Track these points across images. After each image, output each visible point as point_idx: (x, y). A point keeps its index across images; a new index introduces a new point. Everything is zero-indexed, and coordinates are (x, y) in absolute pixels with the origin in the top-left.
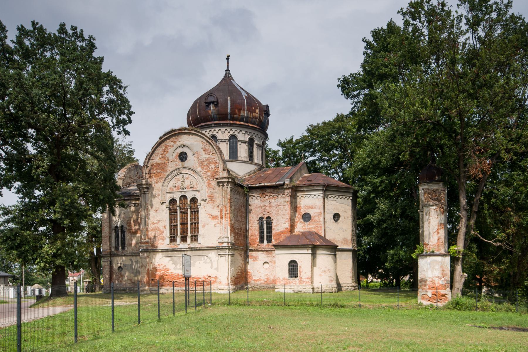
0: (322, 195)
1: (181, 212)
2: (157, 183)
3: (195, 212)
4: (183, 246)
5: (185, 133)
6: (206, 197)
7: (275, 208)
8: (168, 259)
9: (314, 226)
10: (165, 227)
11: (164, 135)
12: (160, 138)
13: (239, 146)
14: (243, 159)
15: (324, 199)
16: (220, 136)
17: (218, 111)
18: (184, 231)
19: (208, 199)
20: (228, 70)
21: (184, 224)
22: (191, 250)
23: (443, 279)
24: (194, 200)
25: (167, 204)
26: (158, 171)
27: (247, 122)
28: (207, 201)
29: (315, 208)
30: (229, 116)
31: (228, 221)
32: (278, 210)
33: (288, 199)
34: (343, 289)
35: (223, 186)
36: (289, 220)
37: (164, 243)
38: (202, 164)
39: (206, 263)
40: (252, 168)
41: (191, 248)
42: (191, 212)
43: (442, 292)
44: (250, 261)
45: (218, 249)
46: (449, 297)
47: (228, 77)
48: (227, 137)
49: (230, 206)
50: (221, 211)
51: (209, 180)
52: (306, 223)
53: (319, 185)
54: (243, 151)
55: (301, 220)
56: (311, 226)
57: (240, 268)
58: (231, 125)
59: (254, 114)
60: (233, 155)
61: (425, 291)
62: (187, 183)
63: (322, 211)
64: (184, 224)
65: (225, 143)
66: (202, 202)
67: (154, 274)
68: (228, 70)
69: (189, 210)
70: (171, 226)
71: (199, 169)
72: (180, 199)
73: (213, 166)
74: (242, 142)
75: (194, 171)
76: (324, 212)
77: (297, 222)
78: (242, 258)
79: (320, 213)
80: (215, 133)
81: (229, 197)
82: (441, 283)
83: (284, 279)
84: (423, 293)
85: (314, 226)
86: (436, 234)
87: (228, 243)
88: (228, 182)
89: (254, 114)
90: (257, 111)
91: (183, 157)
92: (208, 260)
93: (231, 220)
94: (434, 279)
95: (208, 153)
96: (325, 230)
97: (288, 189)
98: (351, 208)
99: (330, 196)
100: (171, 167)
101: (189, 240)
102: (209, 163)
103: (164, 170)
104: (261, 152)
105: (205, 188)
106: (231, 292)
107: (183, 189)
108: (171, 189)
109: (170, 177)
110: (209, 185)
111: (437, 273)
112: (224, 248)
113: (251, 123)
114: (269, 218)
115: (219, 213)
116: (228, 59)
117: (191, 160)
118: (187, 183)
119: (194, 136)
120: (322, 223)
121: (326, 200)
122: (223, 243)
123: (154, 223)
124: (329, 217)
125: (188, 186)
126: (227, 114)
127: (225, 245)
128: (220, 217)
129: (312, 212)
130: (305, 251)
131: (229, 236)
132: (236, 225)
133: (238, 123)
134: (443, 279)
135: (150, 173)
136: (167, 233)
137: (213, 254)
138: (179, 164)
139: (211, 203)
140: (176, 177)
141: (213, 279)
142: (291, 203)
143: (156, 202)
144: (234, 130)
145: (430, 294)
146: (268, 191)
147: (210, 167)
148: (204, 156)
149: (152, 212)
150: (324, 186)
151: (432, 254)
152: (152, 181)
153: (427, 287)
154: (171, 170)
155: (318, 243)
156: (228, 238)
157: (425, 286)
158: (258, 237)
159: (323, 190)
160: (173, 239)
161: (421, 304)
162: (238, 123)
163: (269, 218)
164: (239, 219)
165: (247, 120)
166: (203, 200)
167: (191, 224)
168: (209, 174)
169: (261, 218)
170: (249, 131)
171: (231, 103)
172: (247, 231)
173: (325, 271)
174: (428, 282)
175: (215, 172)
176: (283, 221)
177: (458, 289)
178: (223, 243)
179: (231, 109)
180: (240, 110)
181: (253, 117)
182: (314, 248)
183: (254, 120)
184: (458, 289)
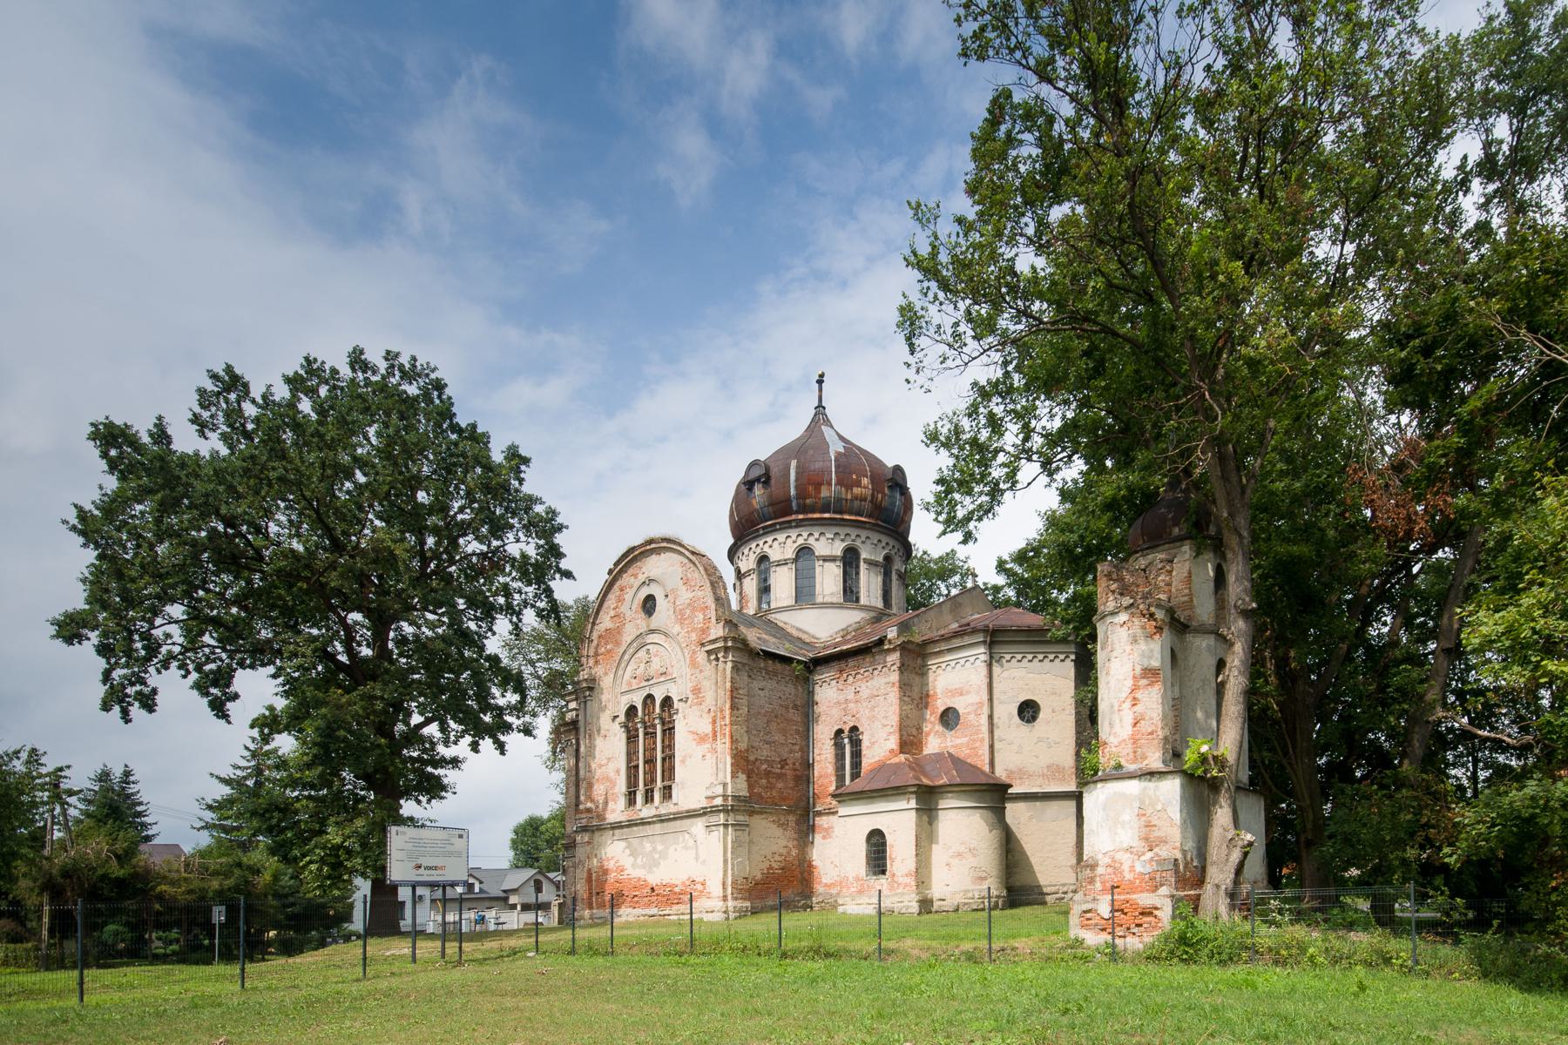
0: (983, 657)
1: (646, 734)
3: (669, 731)
4: (647, 812)
5: (653, 551)
7: (864, 705)
8: (623, 844)
9: (965, 740)
10: (618, 771)
11: (616, 565)
12: (610, 572)
13: (818, 569)
14: (835, 600)
15: (990, 666)
16: (775, 554)
17: (770, 496)
20: (820, 406)
21: (650, 761)
22: (662, 819)
23: (1149, 855)
24: (667, 702)
25: (622, 718)
27: (841, 512)
29: (968, 692)
30: (794, 504)
31: (728, 745)
32: (873, 708)
33: (895, 677)
34: (1048, 898)
35: (717, 659)
36: (896, 728)
37: (617, 811)
38: (681, 619)
39: (686, 848)
40: (852, 617)
42: (664, 731)
43: (1145, 899)
44: (818, 838)
45: (705, 814)
46: (1165, 913)
48: (790, 553)
49: (733, 707)
50: (714, 722)
52: (949, 734)
53: (975, 631)
54: (829, 580)
55: (939, 728)
56: (959, 741)
57: (777, 858)
58: (800, 524)
59: (857, 491)
60: (804, 595)
61: (1089, 898)
62: (656, 665)
63: (985, 697)
64: (650, 761)
65: (785, 568)
67: (602, 883)
68: (820, 406)
69: (659, 728)
70: (629, 768)
71: (676, 629)
73: (701, 616)
74: (826, 559)
75: (666, 634)
76: (991, 700)
77: (928, 734)
78: (790, 833)
79: (981, 704)
80: (766, 548)
81: (728, 685)
82: (1139, 868)
83: (857, 879)
84: (1086, 907)
85: (965, 740)
86: (1127, 705)
87: (725, 797)
88: (726, 649)
89: (857, 491)
90: (865, 481)
91: (649, 605)
92: (691, 843)
93: (733, 741)
94: (1118, 856)
95: (692, 588)
96: (992, 747)
97: (894, 650)
98: (1072, 684)
99: (1008, 657)
100: (629, 633)
101: (657, 796)
103: (618, 644)
104: (880, 579)
105: (687, 670)
106: (732, 916)
108: (630, 684)
109: (627, 657)
110: (693, 664)
111: (1128, 836)
112: (714, 811)
113: (851, 513)
114: (854, 729)
115: (708, 729)
116: (820, 382)
118: (656, 665)
119: (668, 554)
120: (985, 728)
121: (996, 669)
122: (713, 798)
123: (601, 766)
124: (1007, 710)
126: (789, 500)
127: (719, 801)
129: (960, 705)
130: (902, 804)
131: (729, 780)
132: (765, 752)
133: (817, 516)
134: (1149, 855)
135: (596, 654)
136: (621, 786)
137: (698, 825)
141: (699, 887)
142: (904, 686)
143: (605, 720)
144: (805, 535)
145: (1104, 910)
146: (851, 663)
148: (685, 596)
149: (599, 742)
150: (985, 630)
151: (1119, 774)
152: (599, 671)
153: (1098, 885)
155: (944, 780)
156: (725, 785)
157: (1092, 881)
158: (833, 779)
159: (984, 642)
160: (631, 801)
161: (1079, 943)
162: (817, 516)
163: (854, 729)
164: (778, 737)
165: (838, 506)
167: (664, 759)
168: (694, 636)
169: (839, 732)
170: (843, 531)
171: (797, 473)
172: (808, 766)
173: (959, 855)
174: (1100, 870)
176: (882, 734)
177: (1218, 886)
178: (713, 798)
179: (797, 487)
180: (818, 486)
181: (856, 498)
182: (928, 798)
183: (857, 503)
184: (1218, 886)
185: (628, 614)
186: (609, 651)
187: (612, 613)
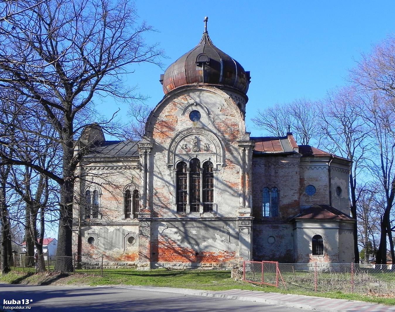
4: (194, 215)
18: (193, 197)
24: (208, 164)
30: (221, 78)
41: (205, 218)
47: (207, 38)
56: (316, 200)
59: (242, 79)
115: (240, 181)
120: (328, 197)
127: (248, 215)
128: (240, 184)
160: (180, 208)
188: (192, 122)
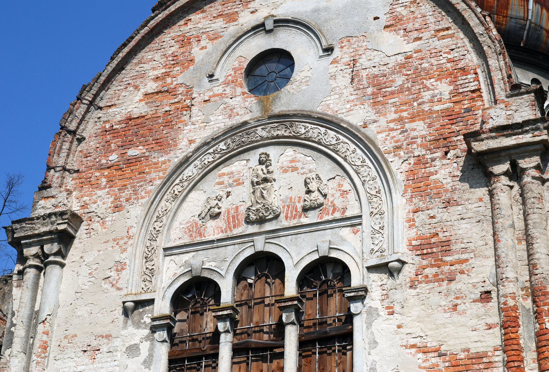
2: (117, 208)
6: (399, 244)
19: (413, 261)
24: (325, 273)
25: (163, 307)
26: (132, 152)
28: (408, 271)
35: (516, 174)
38: (377, 90)
50: (509, 324)
51: (420, 161)
66: (376, 283)
69: (292, 336)
72: (239, 276)
102: (419, 76)
107: (261, 221)
109: (191, 171)
110: (420, 186)
115: (495, 338)
117: (315, 83)
125: (290, 204)
138: (244, 107)
139: (437, 279)
140: (224, 170)
147: (426, 95)
154: (201, 136)
166: (381, 268)
175: (451, 117)
185: (203, 90)
186: (131, 162)
187: (152, 86)
188: (252, 101)
